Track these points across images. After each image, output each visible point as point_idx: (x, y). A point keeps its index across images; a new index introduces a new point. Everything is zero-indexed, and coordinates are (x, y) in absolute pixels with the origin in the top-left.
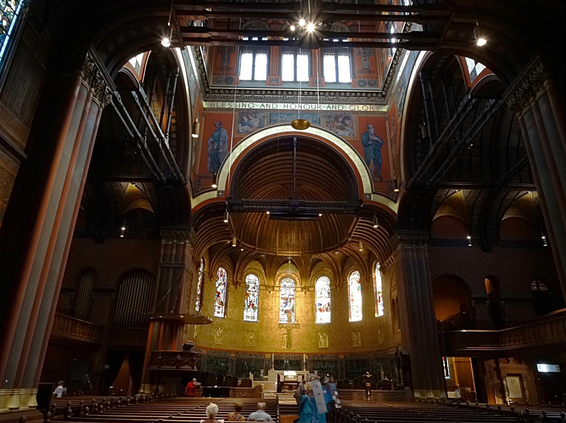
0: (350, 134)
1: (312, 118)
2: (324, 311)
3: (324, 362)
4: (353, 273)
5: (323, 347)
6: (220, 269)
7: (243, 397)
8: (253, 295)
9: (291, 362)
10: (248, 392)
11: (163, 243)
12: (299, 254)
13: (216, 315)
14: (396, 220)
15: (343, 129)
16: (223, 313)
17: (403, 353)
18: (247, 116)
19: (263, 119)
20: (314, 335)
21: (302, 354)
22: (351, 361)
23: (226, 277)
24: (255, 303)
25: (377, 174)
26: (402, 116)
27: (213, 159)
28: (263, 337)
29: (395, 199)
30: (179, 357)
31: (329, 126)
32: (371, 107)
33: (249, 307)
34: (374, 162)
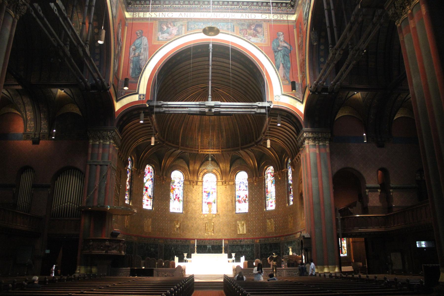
0: (261, 41)
1: (226, 25)
3: (242, 246)
4: (268, 168)
5: (241, 233)
6: (147, 166)
7: (165, 276)
8: (179, 189)
9: (213, 247)
10: (170, 272)
11: (91, 144)
12: (219, 151)
13: (145, 207)
14: (303, 119)
15: (255, 36)
16: (151, 206)
17: (306, 237)
18: (166, 24)
19: (181, 27)
20: (234, 223)
21: (222, 240)
22: (265, 244)
23: (153, 174)
25: (286, 78)
26: (307, 24)
27: (134, 65)
28: (188, 226)
29: (302, 101)
30: (107, 243)
31: (242, 33)
32: (281, 16)
33: (175, 200)
34: (283, 67)
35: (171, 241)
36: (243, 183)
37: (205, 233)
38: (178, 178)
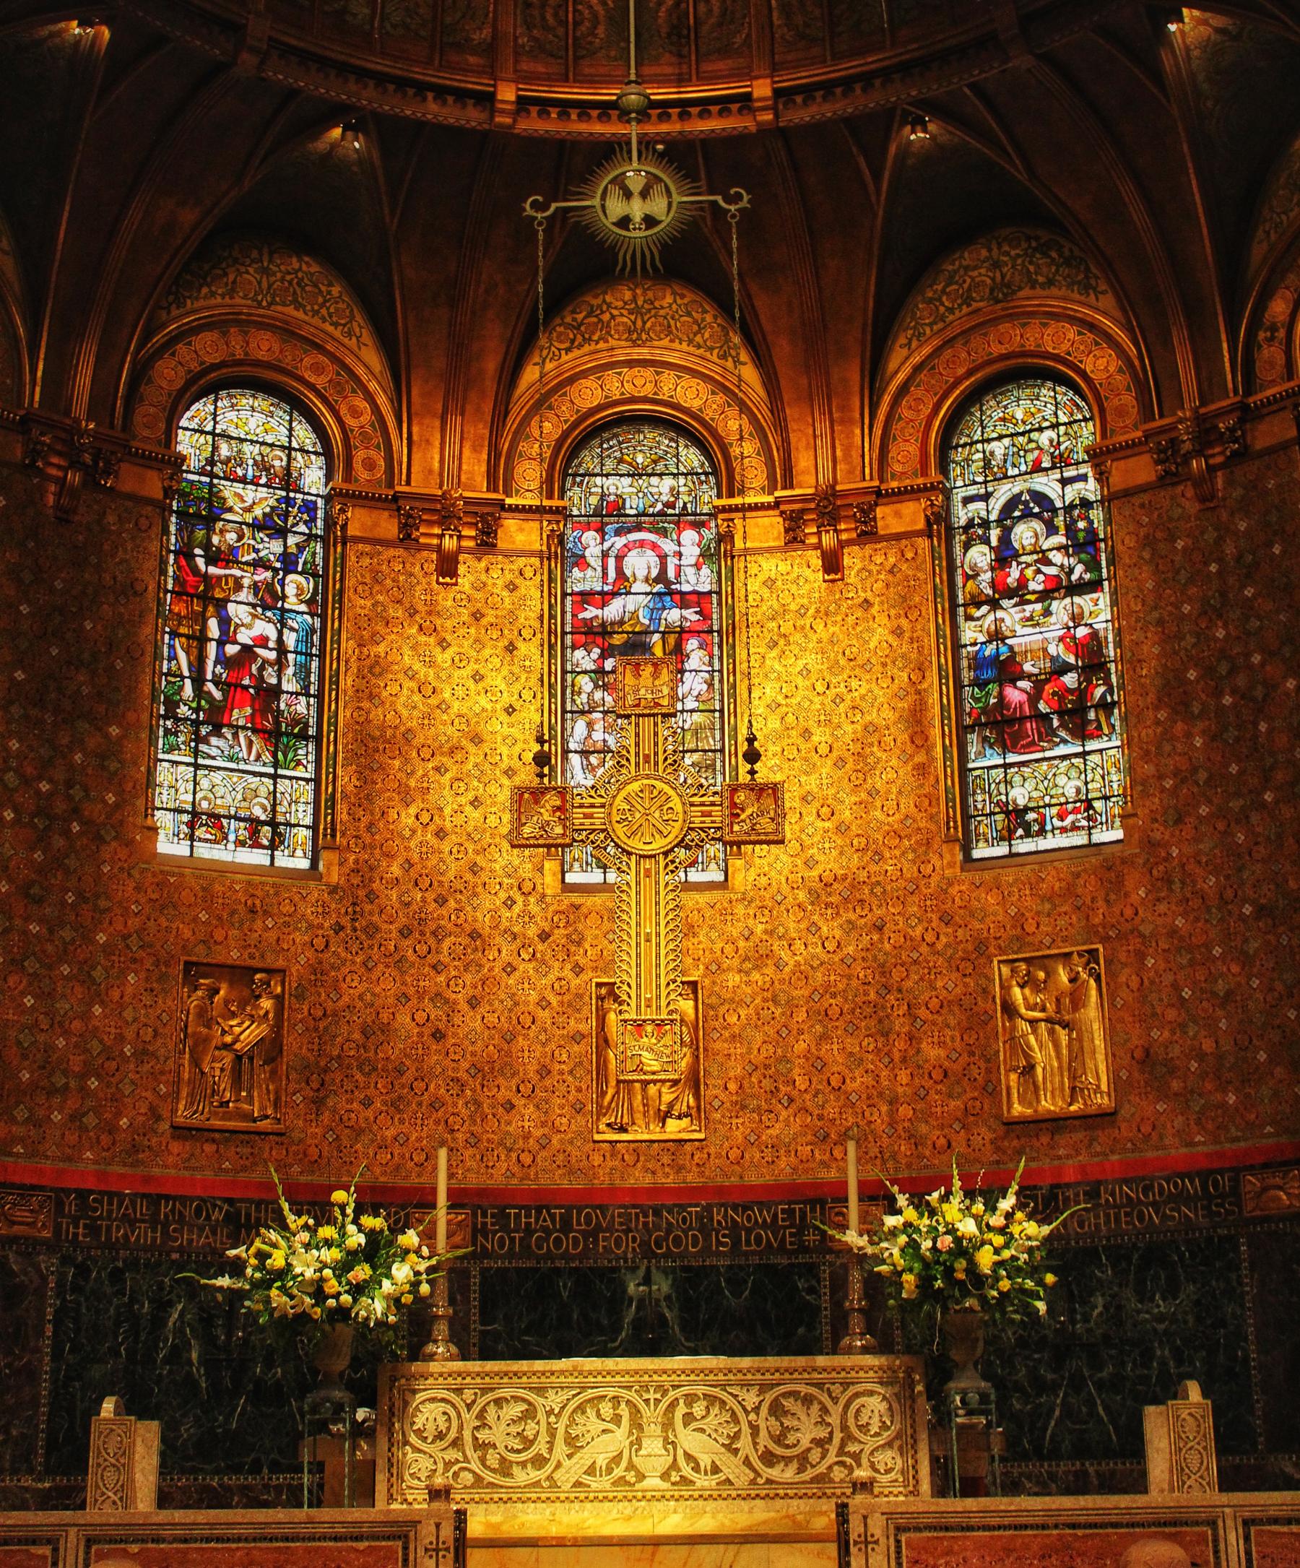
2: (1048, 734)
5: (1047, 1105)
20: (948, 984)
24: (290, 685)
28: (377, 1031)
33: (216, 720)
35: (154, 1221)
36: (1036, 510)
37: (600, 1114)
38: (263, 465)
